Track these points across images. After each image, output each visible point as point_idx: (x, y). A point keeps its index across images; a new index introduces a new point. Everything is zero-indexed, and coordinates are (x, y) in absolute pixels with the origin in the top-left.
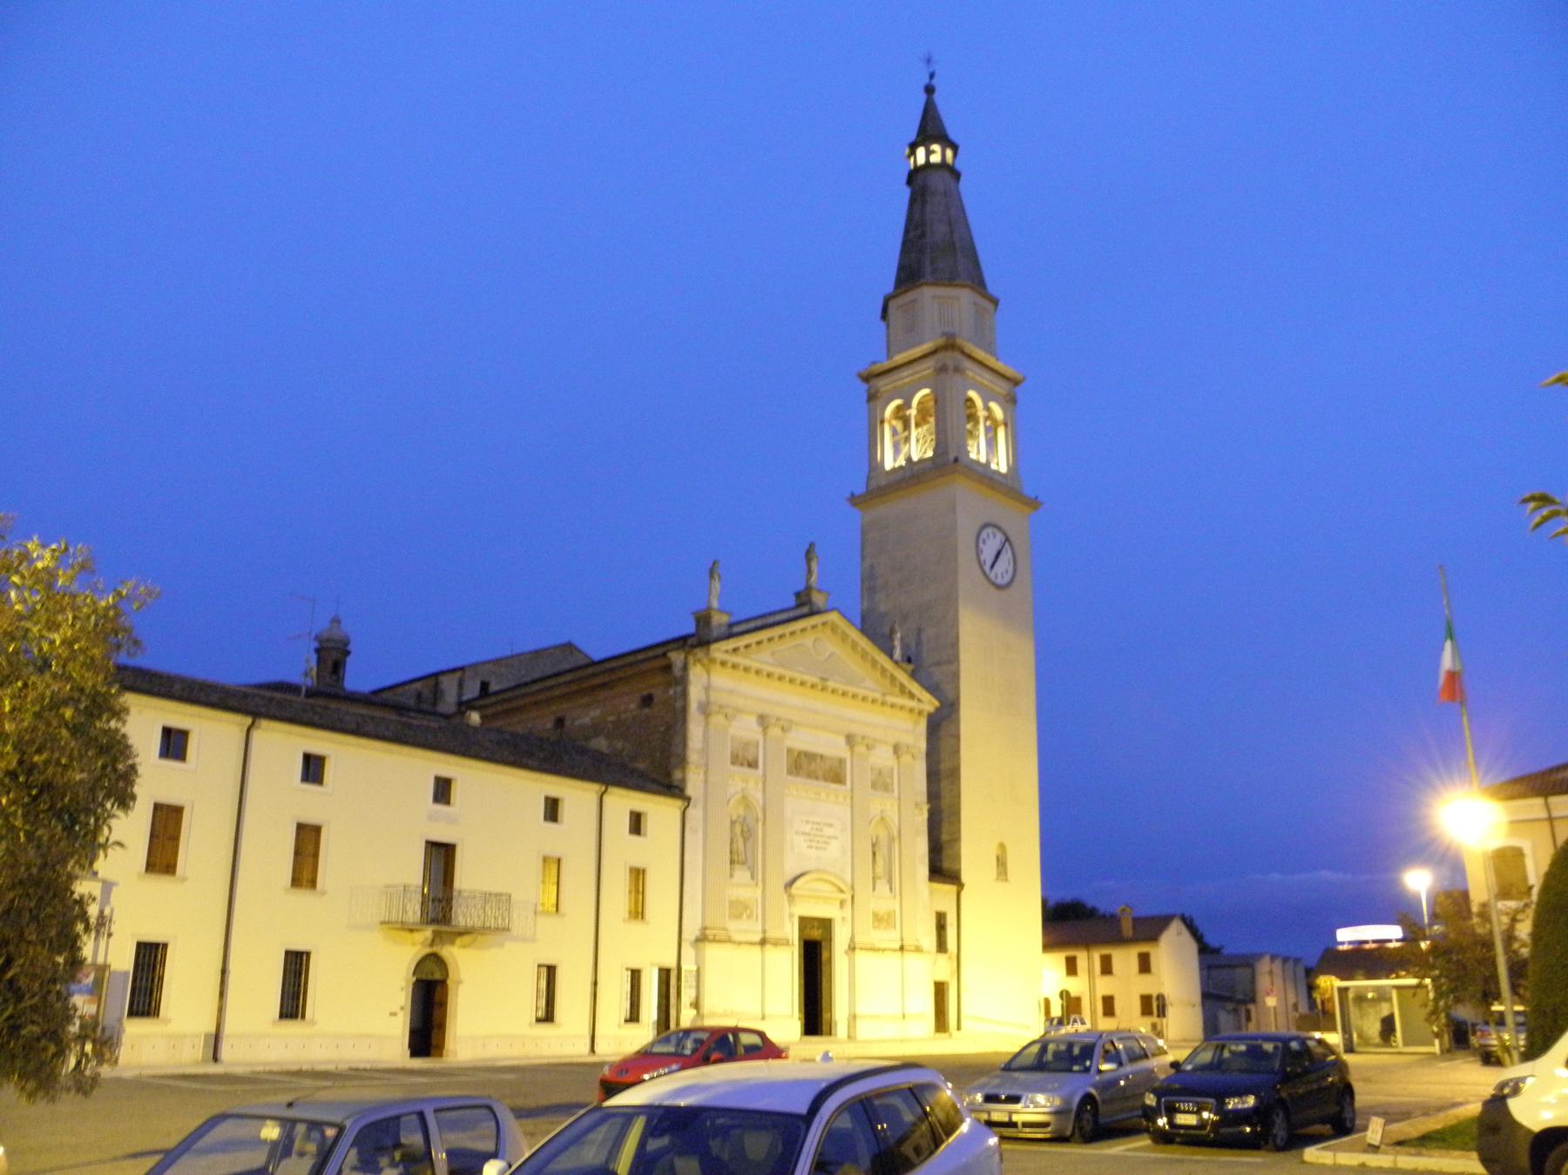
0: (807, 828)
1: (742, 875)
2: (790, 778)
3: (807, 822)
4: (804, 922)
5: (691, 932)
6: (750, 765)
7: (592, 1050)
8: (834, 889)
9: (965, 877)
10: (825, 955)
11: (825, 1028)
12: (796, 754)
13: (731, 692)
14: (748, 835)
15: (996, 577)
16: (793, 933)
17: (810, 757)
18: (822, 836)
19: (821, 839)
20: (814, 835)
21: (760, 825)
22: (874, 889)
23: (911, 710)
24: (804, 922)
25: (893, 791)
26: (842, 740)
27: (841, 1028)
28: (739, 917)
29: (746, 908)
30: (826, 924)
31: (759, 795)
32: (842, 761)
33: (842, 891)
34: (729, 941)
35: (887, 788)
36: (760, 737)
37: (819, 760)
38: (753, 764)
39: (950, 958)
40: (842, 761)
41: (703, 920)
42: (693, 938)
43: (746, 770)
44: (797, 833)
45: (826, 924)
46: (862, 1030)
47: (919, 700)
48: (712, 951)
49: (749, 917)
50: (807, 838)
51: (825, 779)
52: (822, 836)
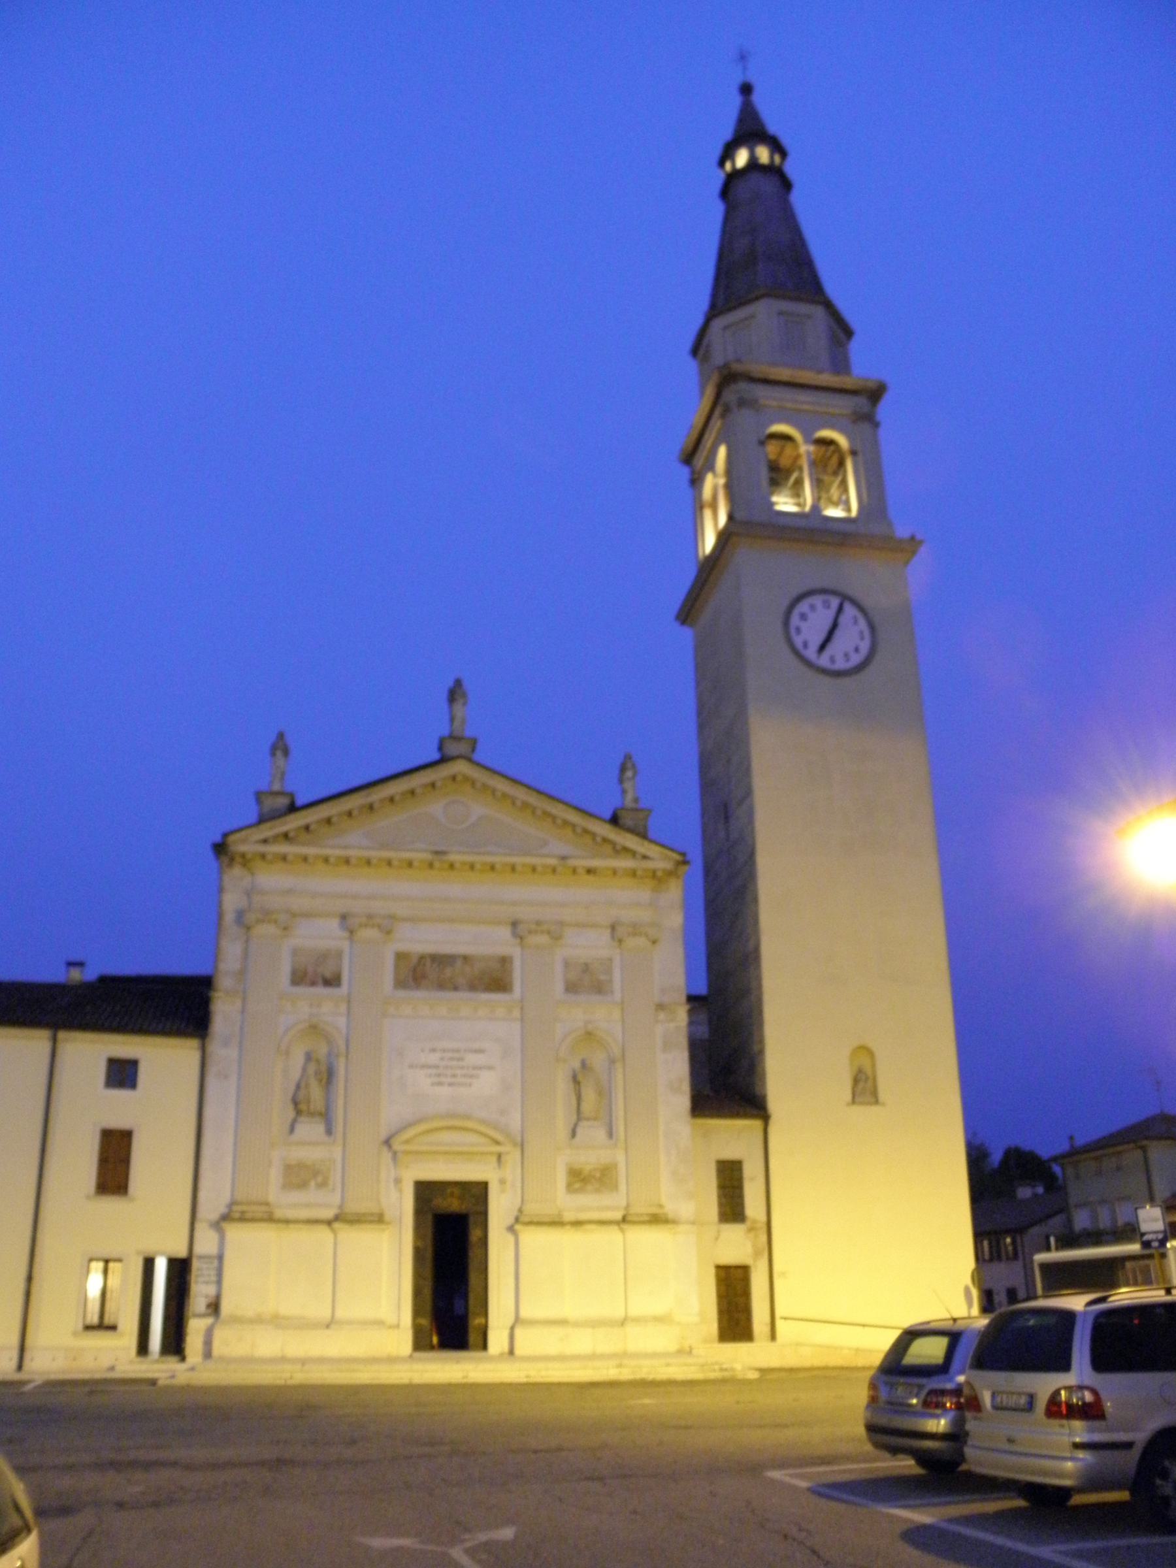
0: (433, 1058)
1: (310, 1129)
2: (401, 993)
3: (433, 1050)
4: (425, 1191)
5: (210, 1208)
6: (327, 983)
7: (20, 1367)
8: (482, 1140)
9: (774, 1103)
10: (475, 1234)
11: (473, 1337)
12: (415, 960)
13: (290, 892)
14: (328, 1077)
15: (832, 659)
16: (405, 1205)
17: (442, 960)
18: (462, 1068)
19: (459, 1072)
20: (446, 1067)
21: (342, 1060)
22: (574, 1134)
23: (633, 873)
24: (425, 1191)
25: (612, 992)
26: (505, 932)
27: (497, 1340)
28: (303, 1185)
29: (316, 1173)
30: (478, 1192)
31: (342, 1022)
32: (505, 961)
33: (497, 1143)
34: (270, 1219)
35: (600, 988)
36: (345, 945)
37: (459, 963)
38: (332, 981)
39: (751, 1230)
40: (505, 961)
41: (232, 1195)
42: (214, 1216)
43: (321, 990)
44: (411, 1066)
45: (478, 1192)
46: (527, 1342)
47: (645, 857)
48: (236, 1233)
49: (323, 1185)
50: (434, 1071)
51: (473, 987)
52: (462, 1068)
